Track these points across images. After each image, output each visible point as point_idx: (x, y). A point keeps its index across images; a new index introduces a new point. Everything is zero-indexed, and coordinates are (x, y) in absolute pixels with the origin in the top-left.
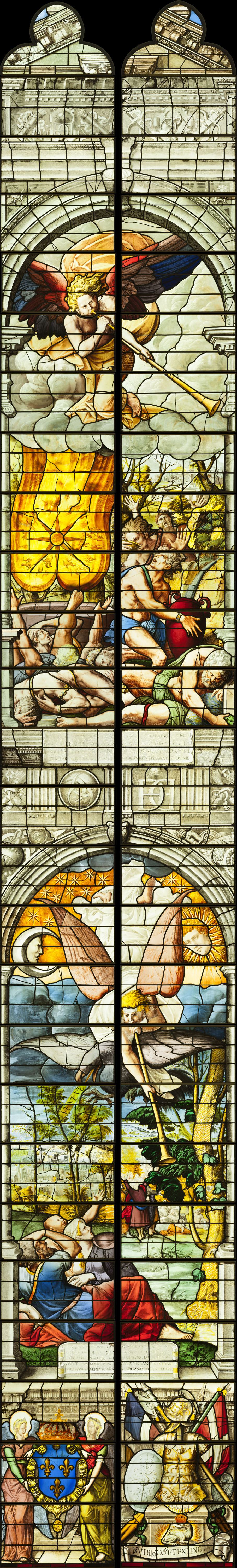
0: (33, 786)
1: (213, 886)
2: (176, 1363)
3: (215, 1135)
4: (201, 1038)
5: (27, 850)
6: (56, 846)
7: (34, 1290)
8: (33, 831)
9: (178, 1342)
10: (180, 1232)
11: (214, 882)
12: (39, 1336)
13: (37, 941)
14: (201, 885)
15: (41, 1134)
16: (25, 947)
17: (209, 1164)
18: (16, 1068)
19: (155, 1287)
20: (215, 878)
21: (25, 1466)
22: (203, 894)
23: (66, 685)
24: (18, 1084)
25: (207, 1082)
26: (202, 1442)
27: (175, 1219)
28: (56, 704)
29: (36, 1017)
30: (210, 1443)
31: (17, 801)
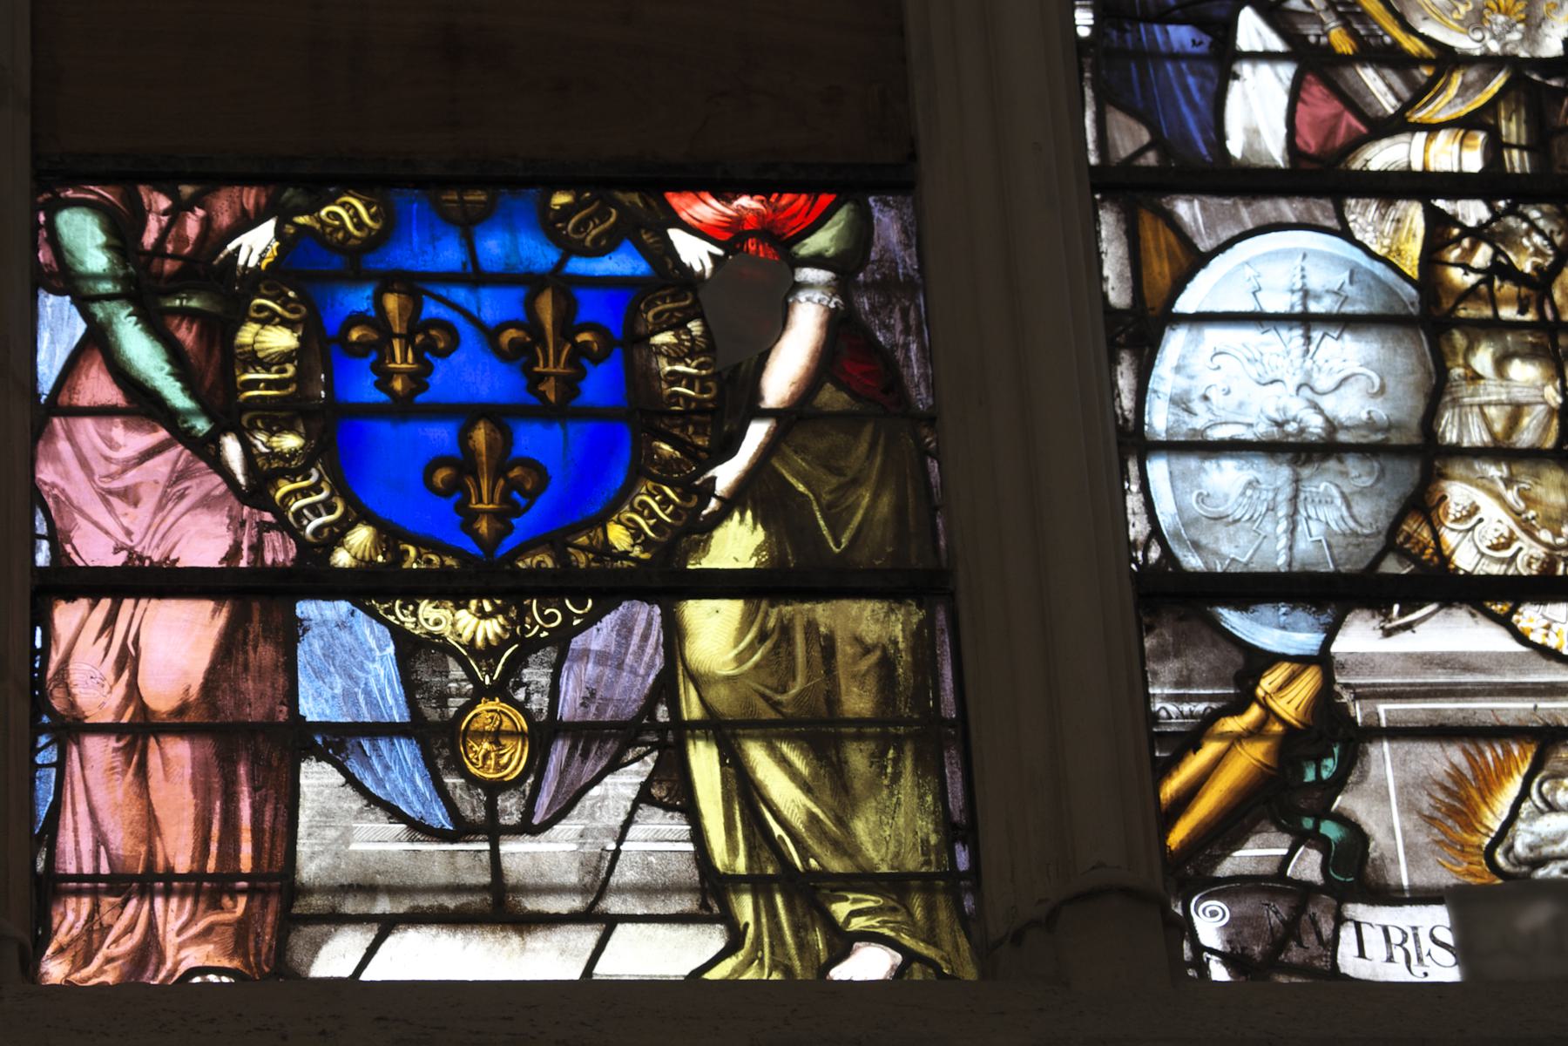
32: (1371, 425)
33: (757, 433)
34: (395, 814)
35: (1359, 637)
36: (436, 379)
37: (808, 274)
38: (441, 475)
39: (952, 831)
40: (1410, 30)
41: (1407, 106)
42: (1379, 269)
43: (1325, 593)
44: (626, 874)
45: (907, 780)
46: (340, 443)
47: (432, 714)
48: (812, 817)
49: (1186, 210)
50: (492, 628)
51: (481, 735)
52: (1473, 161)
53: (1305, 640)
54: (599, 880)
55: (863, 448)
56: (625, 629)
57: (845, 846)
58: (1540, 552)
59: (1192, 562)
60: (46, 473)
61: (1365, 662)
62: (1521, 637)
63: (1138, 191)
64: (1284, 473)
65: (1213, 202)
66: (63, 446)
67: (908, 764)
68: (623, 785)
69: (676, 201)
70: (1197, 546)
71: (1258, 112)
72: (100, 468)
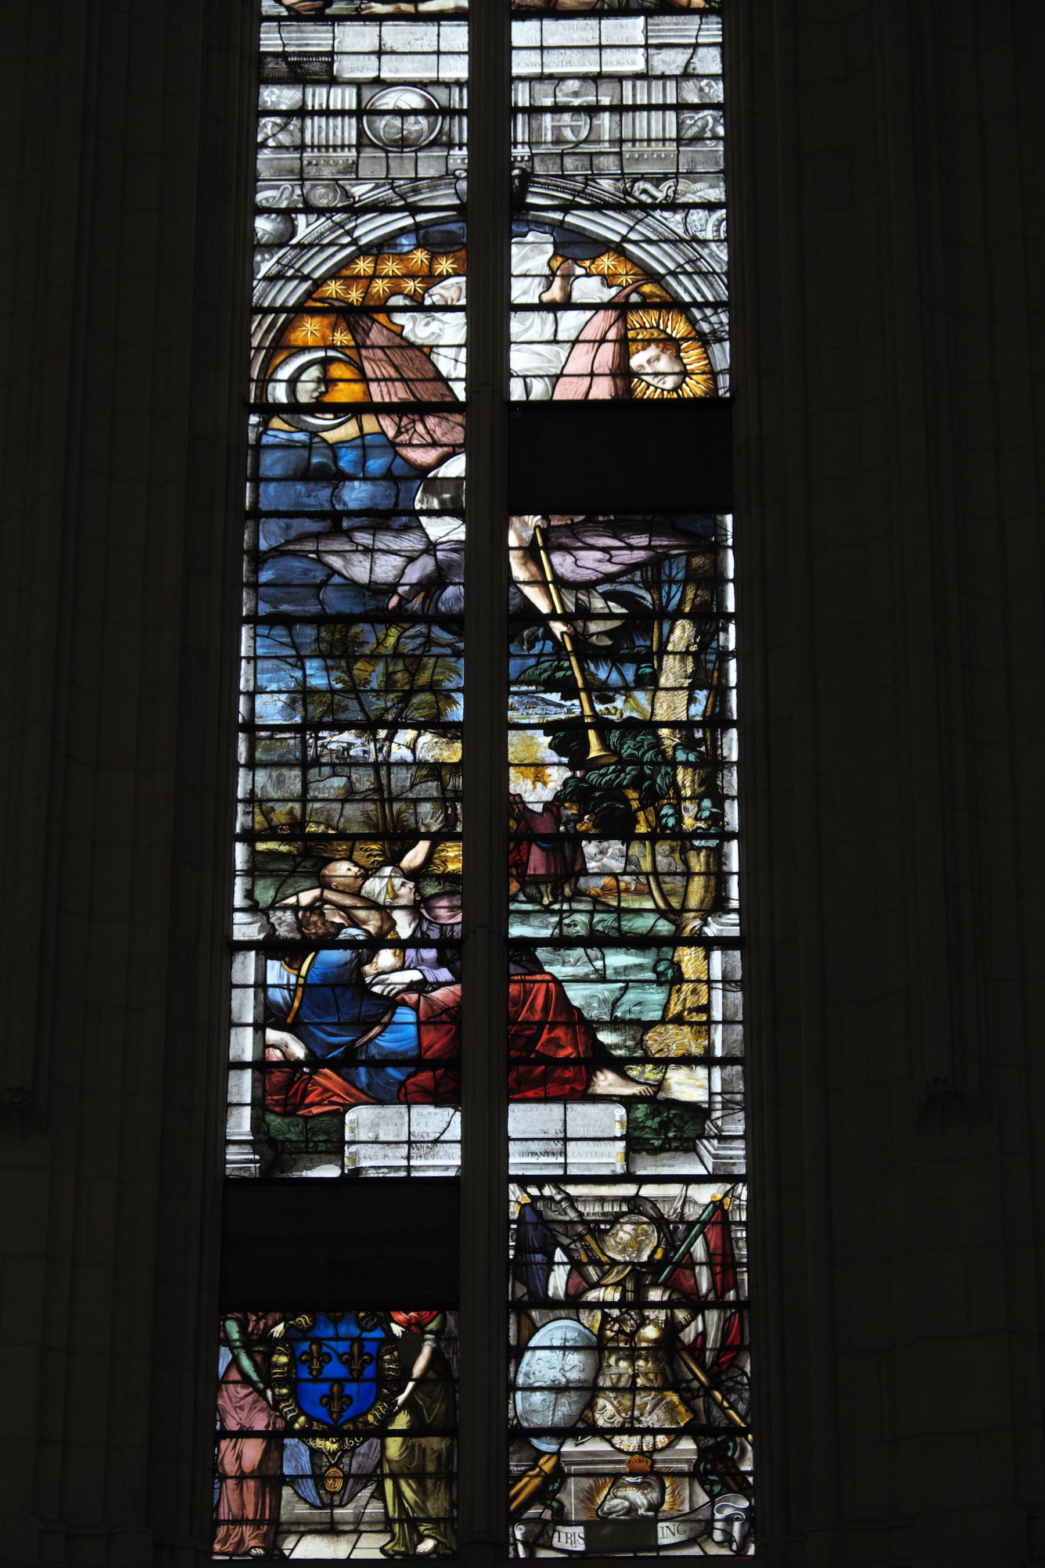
0: (313, 113)
2: (622, 1144)
3: (697, 710)
4: (668, 536)
5: (301, 220)
6: (356, 210)
7: (296, 1004)
8: (314, 187)
9: (627, 1102)
10: (627, 890)
12: (305, 1093)
13: (314, 372)
14: (662, 271)
15: (316, 713)
16: (293, 382)
17: (687, 764)
18: (271, 591)
19: (576, 994)
20: (689, 261)
21: (268, 1356)
24: (273, 620)
25: (678, 614)
26: (679, 1305)
27: (617, 866)
29: (312, 501)
30: (697, 1306)
31: (284, 138)
32: (579, 1381)
33: (411, 1385)
34: (307, 1502)
35: (568, 1447)
36: (325, 1371)
37: (428, 1336)
38: (325, 1400)
39: (453, 1505)
40: (604, 1254)
41: (601, 1279)
42: (587, 1332)
43: (560, 1433)
44: (366, 1519)
45: (442, 1490)
46: (294, 1394)
47: (318, 1472)
48: (416, 1502)
49: (534, 1314)
50: (335, 1446)
51: (330, 1478)
52: (617, 1297)
53: (553, 1448)
54: (358, 1520)
55: (438, 1391)
56: (370, 1446)
57: (424, 1510)
58: (621, 1420)
59: (525, 1424)
60: (220, 1402)
61: (569, 1454)
62: (613, 1446)
63: (522, 1309)
64: (554, 1396)
65: (543, 1311)
66: (225, 1393)
67: (443, 1486)
68: (366, 1493)
69: (393, 1314)
70: (527, 1420)
71: (558, 1281)
72: (234, 1400)
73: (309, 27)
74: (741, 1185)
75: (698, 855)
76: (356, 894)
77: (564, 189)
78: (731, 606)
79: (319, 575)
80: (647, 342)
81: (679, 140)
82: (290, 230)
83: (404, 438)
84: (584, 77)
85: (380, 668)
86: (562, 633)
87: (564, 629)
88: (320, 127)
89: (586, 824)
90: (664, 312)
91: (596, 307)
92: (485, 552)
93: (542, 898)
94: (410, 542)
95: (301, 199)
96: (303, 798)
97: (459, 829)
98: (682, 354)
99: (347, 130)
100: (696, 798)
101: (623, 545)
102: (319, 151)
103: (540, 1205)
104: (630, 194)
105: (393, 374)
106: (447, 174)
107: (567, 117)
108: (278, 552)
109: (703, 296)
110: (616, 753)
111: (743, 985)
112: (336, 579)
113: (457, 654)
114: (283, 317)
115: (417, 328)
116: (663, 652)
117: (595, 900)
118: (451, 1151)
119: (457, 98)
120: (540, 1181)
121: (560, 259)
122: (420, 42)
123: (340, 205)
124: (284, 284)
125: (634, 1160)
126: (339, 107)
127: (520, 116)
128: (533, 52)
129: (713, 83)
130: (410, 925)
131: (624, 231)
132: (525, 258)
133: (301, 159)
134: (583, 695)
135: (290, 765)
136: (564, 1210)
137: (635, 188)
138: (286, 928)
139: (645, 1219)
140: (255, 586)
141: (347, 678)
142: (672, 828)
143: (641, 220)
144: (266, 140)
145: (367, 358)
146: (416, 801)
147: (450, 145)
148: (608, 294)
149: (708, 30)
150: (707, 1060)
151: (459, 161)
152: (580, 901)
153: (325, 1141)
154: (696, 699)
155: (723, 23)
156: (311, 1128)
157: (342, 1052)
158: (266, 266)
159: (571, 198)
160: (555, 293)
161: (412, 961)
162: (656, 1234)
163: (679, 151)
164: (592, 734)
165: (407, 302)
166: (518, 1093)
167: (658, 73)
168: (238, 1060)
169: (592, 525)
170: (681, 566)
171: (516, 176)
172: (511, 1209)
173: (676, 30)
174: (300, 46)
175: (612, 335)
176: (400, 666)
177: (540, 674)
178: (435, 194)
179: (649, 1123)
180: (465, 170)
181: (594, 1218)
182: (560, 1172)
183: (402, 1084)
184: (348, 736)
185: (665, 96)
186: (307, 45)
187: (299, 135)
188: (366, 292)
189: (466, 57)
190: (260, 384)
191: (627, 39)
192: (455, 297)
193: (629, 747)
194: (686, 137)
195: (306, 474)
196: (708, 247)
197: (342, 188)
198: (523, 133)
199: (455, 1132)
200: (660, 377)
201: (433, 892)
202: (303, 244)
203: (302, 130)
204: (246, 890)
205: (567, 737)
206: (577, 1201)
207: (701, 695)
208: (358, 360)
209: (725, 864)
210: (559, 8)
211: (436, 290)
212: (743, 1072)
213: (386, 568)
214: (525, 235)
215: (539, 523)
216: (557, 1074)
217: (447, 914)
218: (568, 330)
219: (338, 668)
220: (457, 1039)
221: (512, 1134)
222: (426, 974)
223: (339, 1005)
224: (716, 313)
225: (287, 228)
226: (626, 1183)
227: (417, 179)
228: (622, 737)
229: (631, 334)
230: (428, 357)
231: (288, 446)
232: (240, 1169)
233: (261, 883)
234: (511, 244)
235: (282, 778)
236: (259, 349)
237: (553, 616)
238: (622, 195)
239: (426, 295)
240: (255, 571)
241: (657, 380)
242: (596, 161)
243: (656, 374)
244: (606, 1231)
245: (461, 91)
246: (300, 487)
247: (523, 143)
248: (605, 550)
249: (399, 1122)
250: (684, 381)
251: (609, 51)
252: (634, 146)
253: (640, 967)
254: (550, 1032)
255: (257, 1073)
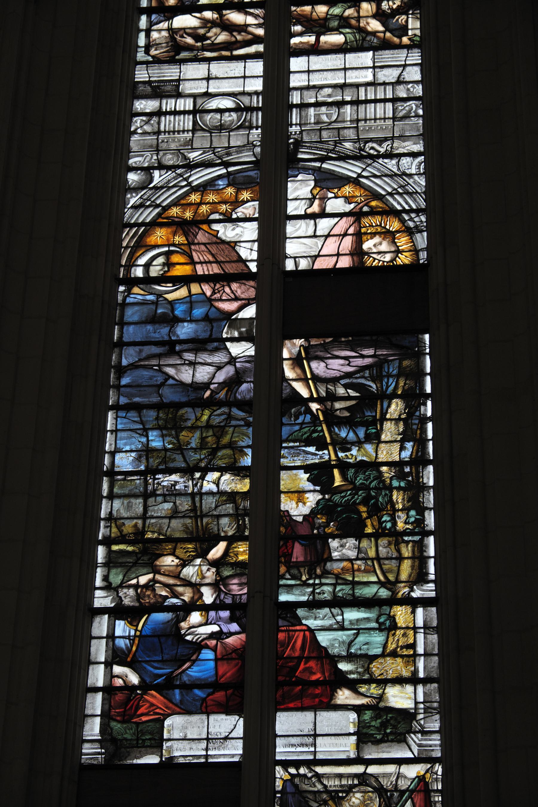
0: (166, 113)
1: (398, 193)
2: (354, 738)
3: (406, 455)
5: (156, 173)
7: (134, 648)
8: (165, 154)
11: (400, 190)
13: (161, 260)
14: (383, 193)
16: (147, 266)
17: (399, 489)
18: (128, 390)
22: (386, 203)
23: (213, 24)
24: (127, 408)
25: (394, 395)
27: (352, 554)
28: (197, 42)
29: (157, 335)
31: (147, 128)
73: (165, 66)
74: (437, 764)
75: (407, 546)
76: (177, 576)
77: (321, 149)
78: (428, 389)
79: (160, 379)
80: (373, 235)
81: (394, 118)
82: (149, 179)
83: (217, 296)
84: (334, 86)
85: (197, 434)
86: (317, 410)
87: (319, 407)
88: (170, 121)
89: (332, 528)
90: (384, 217)
91: (341, 215)
92: (267, 362)
93: (301, 576)
94: (219, 358)
95: (157, 161)
96: (144, 517)
97: (247, 533)
98: (396, 241)
99: (188, 122)
100: (406, 510)
101: (357, 355)
102: (169, 134)
103: (297, 780)
104: (363, 150)
105: (211, 259)
106: (248, 144)
107: (324, 109)
108: (133, 366)
109: (410, 206)
110: (352, 483)
111: (437, 630)
112: (171, 382)
113: (248, 424)
114: (143, 228)
115: (227, 232)
116: (383, 418)
117: (337, 577)
118: (236, 745)
119: (255, 101)
120: (297, 764)
121: (318, 189)
122: (233, 72)
123: (181, 164)
124: (144, 210)
125: (362, 749)
126: (182, 109)
127: (294, 110)
128: (303, 74)
129: (416, 86)
130: (212, 596)
131: (359, 171)
132: (296, 189)
133: (157, 139)
134: (330, 448)
135: (136, 496)
136: (314, 784)
137: (366, 147)
138: (129, 599)
139: (370, 789)
140: (118, 387)
141: (175, 441)
142: (389, 530)
143: (370, 165)
144: (136, 129)
145: (194, 250)
146: (219, 517)
147: (251, 127)
148: (348, 208)
149: (412, 56)
150: (414, 680)
151: (256, 136)
152: (327, 578)
153: (150, 739)
154: (405, 447)
155: (421, 53)
156: (140, 731)
157: (164, 680)
158: (133, 200)
159: (326, 154)
160: (315, 208)
161: (213, 619)
162: (378, 799)
163: (394, 125)
164: (336, 472)
165: (221, 217)
166: (283, 704)
167: (381, 81)
168: (93, 686)
169: (338, 343)
170: (395, 366)
171: (291, 143)
172: (277, 784)
173: (393, 58)
174: (159, 77)
175: (351, 231)
176: (210, 433)
177: (302, 435)
178: (241, 155)
179: (373, 723)
180: (259, 141)
181: (334, 789)
182: (311, 757)
183: (204, 700)
184: (174, 477)
185: (385, 94)
186: (164, 76)
187: (157, 126)
188: (196, 213)
189: (262, 79)
190: (127, 268)
191: (362, 64)
192: (252, 213)
193: (361, 479)
194: (398, 116)
195: (154, 320)
196: (412, 178)
197: (183, 154)
198: (296, 119)
199: (239, 732)
200: (382, 255)
201: (228, 574)
202: (157, 187)
203: (159, 123)
204: (104, 576)
205: (319, 474)
206: (323, 777)
207: (409, 445)
208: (189, 252)
209: (425, 551)
210: (319, 49)
211: (240, 209)
212: (438, 687)
213: (203, 374)
214: (296, 176)
215: (303, 343)
216: (310, 692)
217: (237, 588)
218: (323, 229)
219: (169, 436)
220: (242, 670)
221: (278, 732)
222: (222, 627)
223: (163, 649)
224: (418, 216)
225: (147, 178)
226: (357, 764)
227: (229, 147)
228: (356, 473)
229: (363, 230)
230: (234, 248)
231: (144, 303)
232: (91, 759)
233: (113, 571)
234: (287, 182)
235: (130, 504)
236: (126, 247)
237: (312, 399)
238: (358, 151)
239: (233, 213)
240: (119, 378)
241: (380, 256)
242: (342, 132)
243: (379, 253)
244: (343, 798)
245: (258, 98)
246: (149, 327)
247: (296, 124)
248: (346, 358)
249: (201, 726)
250: (397, 256)
251: (350, 71)
252: (366, 123)
253: (368, 620)
254: (305, 663)
255: (106, 694)
